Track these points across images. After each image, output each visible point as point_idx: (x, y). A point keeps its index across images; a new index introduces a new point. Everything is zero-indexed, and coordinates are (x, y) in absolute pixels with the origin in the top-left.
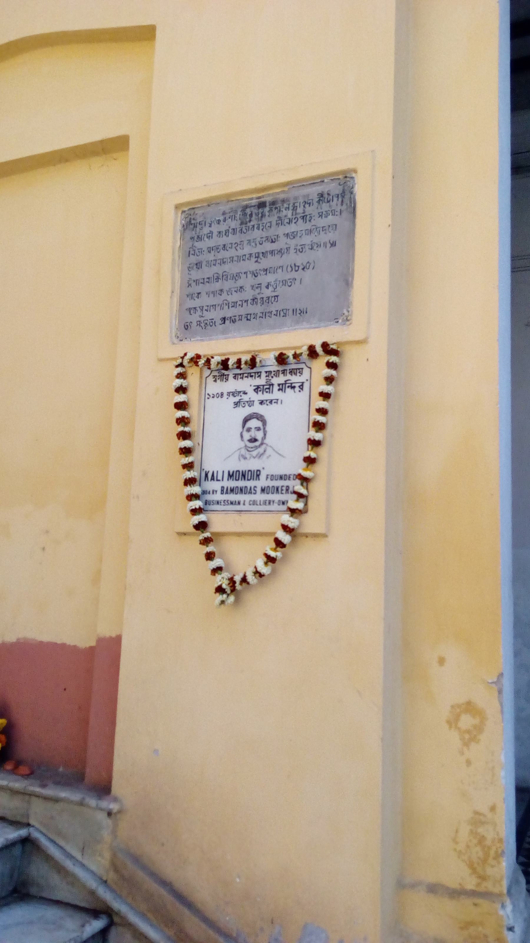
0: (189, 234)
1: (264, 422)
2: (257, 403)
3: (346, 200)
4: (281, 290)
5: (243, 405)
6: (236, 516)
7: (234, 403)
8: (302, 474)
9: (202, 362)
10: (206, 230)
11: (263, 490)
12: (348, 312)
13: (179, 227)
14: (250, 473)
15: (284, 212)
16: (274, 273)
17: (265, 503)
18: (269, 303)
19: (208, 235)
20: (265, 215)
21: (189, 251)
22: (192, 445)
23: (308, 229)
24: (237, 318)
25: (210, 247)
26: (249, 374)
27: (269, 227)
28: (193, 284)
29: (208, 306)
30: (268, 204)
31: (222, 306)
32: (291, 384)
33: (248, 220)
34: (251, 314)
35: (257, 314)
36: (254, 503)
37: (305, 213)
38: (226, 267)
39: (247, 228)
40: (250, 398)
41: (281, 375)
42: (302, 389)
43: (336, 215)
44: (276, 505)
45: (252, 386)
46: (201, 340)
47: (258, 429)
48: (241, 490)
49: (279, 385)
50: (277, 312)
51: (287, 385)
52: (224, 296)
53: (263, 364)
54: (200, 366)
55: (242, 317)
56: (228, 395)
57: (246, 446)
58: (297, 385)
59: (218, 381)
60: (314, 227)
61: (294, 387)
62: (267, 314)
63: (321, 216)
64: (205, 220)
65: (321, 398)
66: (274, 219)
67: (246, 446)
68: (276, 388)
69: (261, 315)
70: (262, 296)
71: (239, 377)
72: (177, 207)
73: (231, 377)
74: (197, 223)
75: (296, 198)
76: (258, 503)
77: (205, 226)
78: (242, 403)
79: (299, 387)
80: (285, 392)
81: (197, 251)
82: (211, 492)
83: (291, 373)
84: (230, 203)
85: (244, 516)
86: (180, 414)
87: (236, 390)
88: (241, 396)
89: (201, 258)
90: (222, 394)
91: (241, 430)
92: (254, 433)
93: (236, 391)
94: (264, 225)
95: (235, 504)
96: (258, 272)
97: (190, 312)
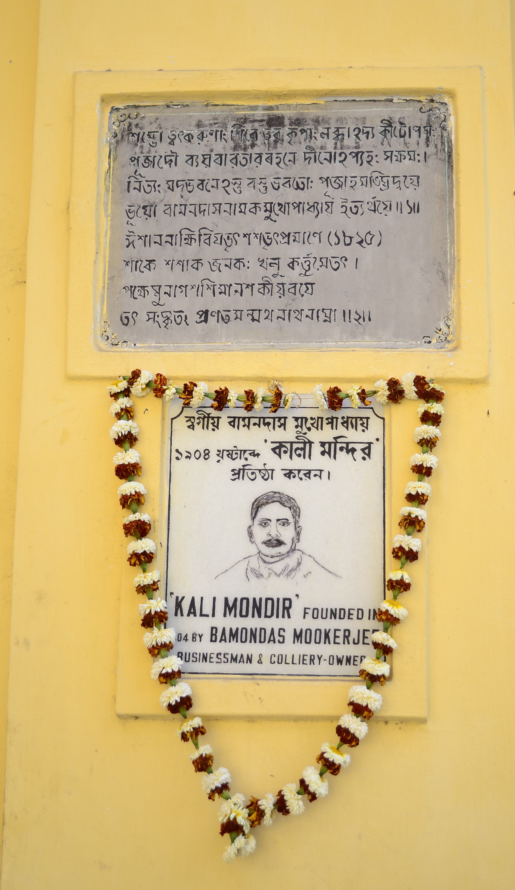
1: (296, 511)
2: (279, 475)
3: (435, 138)
4: (315, 274)
5: (252, 477)
6: (248, 685)
7: (233, 470)
8: (392, 612)
9: (170, 392)
10: (163, 149)
13: (107, 136)
14: (269, 602)
16: (304, 243)
18: (295, 294)
19: (168, 159)
20: (283, 140)
21: (129, 182)
23: (367, 177)
25: (173, 181)
26: (262, 420)
27: (290, 161)
28: (139, 243)
29: (170, 286)
30: (287, 122)
31: (201, 287)
32: (347, 444)
33: (248, 143)
34: (260, 311)
35: (272, 311)
36: (281, 660)
37: (359, 148)
39: (248, 157)
40: (265, 464)
41: (327, 427)
42: (369, 455)
43: (416, 160)
44: (324, 664)
46: (155, 347)
47: (285, 522)
49: (323, 444)
50: (312, 313)
52: (204, 271)
55: (241, 313)
56: (218, 455)
57: (259, 552)
58: (358, 447)
59: (198, 428)
61: (353, 450)
62: (293, 315)
63: (389, 156)
64: (160, 131)
65: (416, 476)
66: (301, 150)
68: (317, 449)
69: (281, 314)
70: (279, 280)
71: (242, 423)
72: (104, 100)
73: (224, 422)
74: (144, 133)
75: (339, 120)
76: (289, 660)
77: (161, 140)
78: (250, 472)
79: (363, 450)
80: (335, 458)
81: (144, 184)
82: (190, 637)
83: (345, 425)
84: (210, 108)
87: (235, 447)
88: (246, 459)
89: (153, 197)
90: (207, 454)
91: (250, 523)
93: (236, 449)
94: (282, 156)
95: (241, 661)
96: (271, 236)
97: (132, 293)
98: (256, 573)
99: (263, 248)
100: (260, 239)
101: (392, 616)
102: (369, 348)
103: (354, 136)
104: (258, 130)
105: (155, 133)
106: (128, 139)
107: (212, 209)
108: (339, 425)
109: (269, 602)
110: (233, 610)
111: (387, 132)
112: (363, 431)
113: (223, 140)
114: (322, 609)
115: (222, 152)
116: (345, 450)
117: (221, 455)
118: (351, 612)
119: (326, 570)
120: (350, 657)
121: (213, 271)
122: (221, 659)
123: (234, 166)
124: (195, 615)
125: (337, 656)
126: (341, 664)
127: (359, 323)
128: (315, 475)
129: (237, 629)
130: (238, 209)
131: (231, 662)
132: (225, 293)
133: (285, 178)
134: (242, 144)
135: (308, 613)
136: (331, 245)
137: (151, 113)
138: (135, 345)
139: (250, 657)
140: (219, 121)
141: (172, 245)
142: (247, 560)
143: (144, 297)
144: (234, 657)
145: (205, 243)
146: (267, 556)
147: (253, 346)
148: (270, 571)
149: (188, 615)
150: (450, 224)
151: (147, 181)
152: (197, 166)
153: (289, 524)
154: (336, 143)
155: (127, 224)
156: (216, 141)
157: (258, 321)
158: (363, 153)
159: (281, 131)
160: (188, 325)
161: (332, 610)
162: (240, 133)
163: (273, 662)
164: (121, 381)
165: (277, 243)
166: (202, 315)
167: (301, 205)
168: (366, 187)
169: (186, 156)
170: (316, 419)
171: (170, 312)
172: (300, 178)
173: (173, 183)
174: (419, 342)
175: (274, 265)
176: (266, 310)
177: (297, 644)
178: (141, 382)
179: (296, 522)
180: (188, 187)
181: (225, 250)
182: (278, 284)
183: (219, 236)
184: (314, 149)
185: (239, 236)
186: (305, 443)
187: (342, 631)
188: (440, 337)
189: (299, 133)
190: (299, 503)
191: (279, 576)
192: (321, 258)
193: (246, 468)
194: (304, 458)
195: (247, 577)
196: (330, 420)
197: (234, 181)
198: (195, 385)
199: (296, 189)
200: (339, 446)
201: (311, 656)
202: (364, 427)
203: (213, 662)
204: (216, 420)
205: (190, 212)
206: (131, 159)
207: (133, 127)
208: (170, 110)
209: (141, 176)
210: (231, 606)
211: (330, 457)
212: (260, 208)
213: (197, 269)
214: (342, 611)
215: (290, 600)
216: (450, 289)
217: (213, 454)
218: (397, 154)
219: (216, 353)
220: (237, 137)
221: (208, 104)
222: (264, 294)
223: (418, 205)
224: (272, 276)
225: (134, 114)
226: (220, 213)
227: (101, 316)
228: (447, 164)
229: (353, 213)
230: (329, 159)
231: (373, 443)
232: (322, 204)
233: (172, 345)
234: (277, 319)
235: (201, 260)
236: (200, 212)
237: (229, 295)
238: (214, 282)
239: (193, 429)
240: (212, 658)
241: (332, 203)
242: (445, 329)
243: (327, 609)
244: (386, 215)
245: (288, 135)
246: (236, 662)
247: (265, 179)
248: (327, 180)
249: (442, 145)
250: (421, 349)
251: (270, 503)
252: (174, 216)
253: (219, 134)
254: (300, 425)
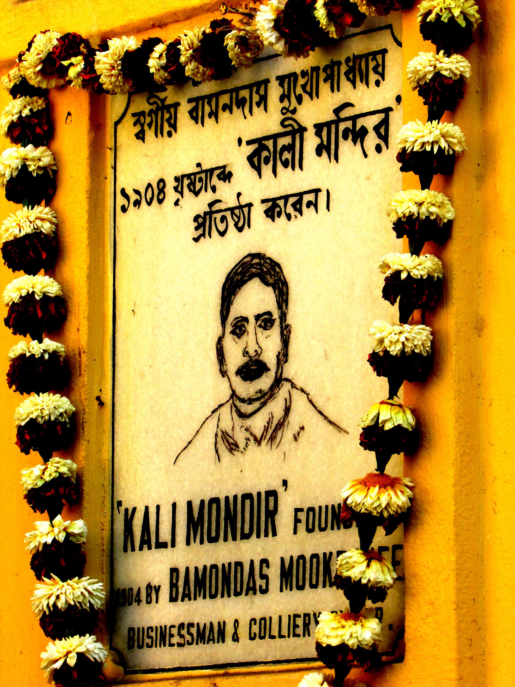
32: (354, 118)
40: (239, 194)
49: (319, 128)
51: (342, 126)
57: (234, 394)
67: (234, 394)
78: (218, 216)
79: (376, 129)
91: (215, 328)
93: (198, 170)
98: (228, 442)
129: (205, 567)
142: (216, 415)
163: (253, 636)
194: (293, 168)
195: (217, 451)
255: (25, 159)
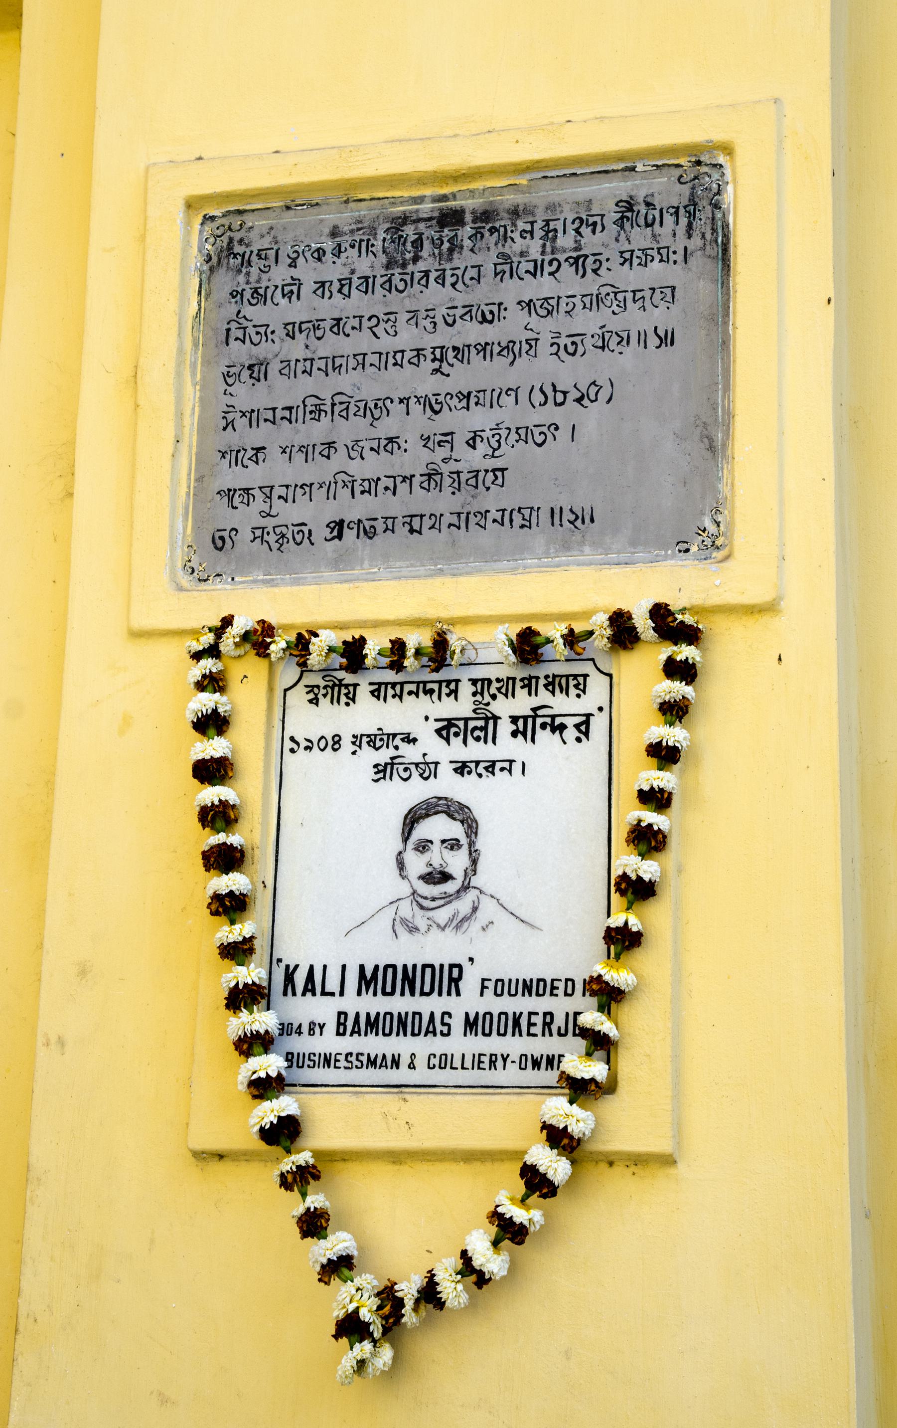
0: (225, 281)
1: (471, 826)
2: (446, 770)
3: (702, 223)
4: (509, 455)
5: (405, 775)
6: (390, 1101)
7: (376, 766)
8: (607, 978)
9: (277, 647)
10: (280, 274)
11: (471, 1024)
12: (718, 524)
13: (195, 260)
14: (428, 971)
15: (519, 244)
16: (491, 407)
17: (477, 1062)
18: (476, 487)
19: (287, 289)
20: (462, 247)
21: (228, 330)
22: (250, 887)
23: (592, 295)
24: (380, 526)
25: (294, 323)
26: (421, 686)
27: (472, 279)
28: (241, 423)
29: (287, 486)
30: (468, 217)
31: (333, 485)
32: (553, 717)
33: (408, 256)
34: (422, 516)
35: (441, 515)
36: (444, 1062)
37: (580, 249)
38: (345, 382)
39: (408, 278)
40: (425, 755)
41: (521, 693)
42: (586, 734)
43: (671, 262)
44: (512, 1068)
45: (431, 720)
46: (264, 582)
47: (453, 844)
48: (402, 1023)
49: (514, 719)
50: (503, 515)
52: (339, 460)
53: (471, 654)
54: (273, 655)
55: (393, 522)
56: (354, 743)
57: (414, 892)
58: (570, 722)
59: (324, 702)
60: (609, 289)
61: (562, 727)
63: (627, 259)
64: (275, 247)
65: (654, 761)
66: (489, 260)
67: (414, 892)
68: (505, 728)
70: (453, 466)
71: (390, 692)
72: (190, 205)
73: (364, 692)
74: (252, 252)
75: (551, 207)
76: (457, 1063)
77: (277, 262)
78: (401, 767)
79: (577, 726)
80: (533, 740)
81: (251, 331)
82: (305, 1029)
83: (550, 688)
85: (417, 1102)
86: (212, 794)
87: (380, 729)
88: (396, 748)
90: (337, 741)
91: (401, 847)
92: (437, 857)
93: (380, 732)
94: (459, 273)
96: (441, 399)
97: (231, 500)
98: (407, 926)
99: (429, 418)
100: (425, 405)
101: (607, 983)
102: (591, 564)
103: (573, 232)
104: (423, 234)
105: (268, 252)
106: (228, 263)
107: (352, 363)
108: (541, 688)
109: (428, 971)
110: (373, 984)
111: (625, 219)
112: (578, 696)
113: (370, 254)
114: (510, 980)
115: (368, 273)
116: (549, 728)
117: (358, 743)
118: (556, 984)
119: (517, 917)
120: (553, 1056)
121: (353, 459)
122: (351, 1062)
123: (387, 293)
124: (314, 994)
125: (532, 1055)
126: (539, 1069)
127: (576, 527)
128: (502, 769)
129: (378, 1014)
130: (391, 361)
131: (367, 1068)
132: (369, 492)
133: (464, 307)
134: (399, 258)
135: (487, 988)
136: (534, 407)
137: (264, 220)
138: (233, 579)
139: (397, 1058)
140: (365, 225)
141: (291, 422)
142: (395, 906)
143: (248, 505)
144: (372, 1059)
145: (341, 416)
146: (426, 898)
147: (410, 571)
148: (430, 922)
149: (304, 994)
150: (722, 359)
151: (255, 326)
152: (330, 298)
153: (460, 846)
154: (544, 246)
155: (225, 394)
156: (360, 256)
157: (420, 533)
158: (586, 256)
159: (460, 233)
160: (313, 544)
161: (524, 981)
162: (397, 240)
163: (431, 1066)
164: (206, 634)
165: (451, 410)
166: (335, 527)
167: (489, 348)
168: (591, 310)
169: (315, 283)
170: (505, 680)
171: (286, 526)
172: (487, 305)
173: (294, 327)
174: (670, 552)
175: (446, 444)
176: (431, 515)
177: (471, 1038)
178: (233, 633)
179: (471, 844)
180: (317, 331)
181: (371, 425)
182: (450, 473)
183: (363, 404)
184: (510, 258)
185: (392, 402)
186: (487, 719)
187: (541, 1015)
188: (703, 541)
189: (487, 234)
190: (477, 813)
191: (443, 929)
192: (518, 429)
193: (395, 761)
194: (486, 742)
195: (394, 931)
196: (526, 682)
197: (386, 318)
198: (316, 635)
199: (481, 323)
200: (539, 721)
201: (491, 1055)
202: (580, 689)
203: (340, 1068)
204: (351, 689)
205: (319, 369)
206: (231, 294)
207: (236, 243)
208: (291, 212)
209: (247, 319)
210: (368, 978)
211: (526, 739)
212: (424, 356)
213: (328, 457)
214: (542, 984)
215: (460, 967)
216: (722, 463)
217: (346, 741)
218: (640, 253)
219: (351, 585)
220: (391, 247)
221: (348, 199)
222: (429, 491)
223: (673, 333)
224: (442, 460)
225: (236, 225)
226: (363, 368)
227: (183, 537)
228: (720, 262)
229: (569, 354)
230: (532, 271)
231: (593, 715)
232: (521, 342)
233: (288, 576)
234: (449, 527)
235: (334, 442)
236: (334, 369)
237: (376, 496)
238: (353, 476)
239: (317, 704)
240: (339, 1061)
241: (537, 340)
242: (712, 528)
243: (517, 980)
244: (621, 353)
245: (470, 238)
246: (375, 1068)
247: (434, 309)
248: (528, 305)
249: (712, 234)
250: (672, 562)
251: (432, 815)
252: (295, 377)
253: (364, 244)
254: (479, 691)
255: (216, 703)
